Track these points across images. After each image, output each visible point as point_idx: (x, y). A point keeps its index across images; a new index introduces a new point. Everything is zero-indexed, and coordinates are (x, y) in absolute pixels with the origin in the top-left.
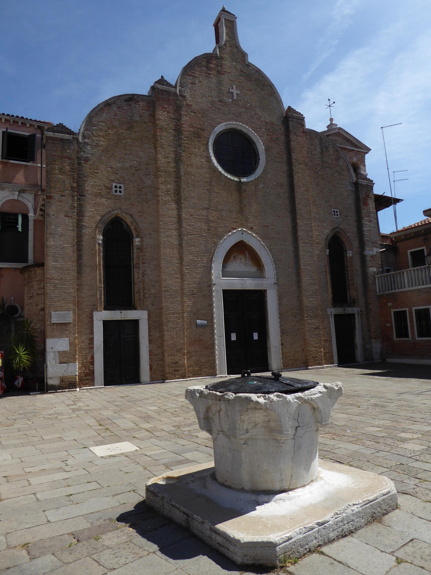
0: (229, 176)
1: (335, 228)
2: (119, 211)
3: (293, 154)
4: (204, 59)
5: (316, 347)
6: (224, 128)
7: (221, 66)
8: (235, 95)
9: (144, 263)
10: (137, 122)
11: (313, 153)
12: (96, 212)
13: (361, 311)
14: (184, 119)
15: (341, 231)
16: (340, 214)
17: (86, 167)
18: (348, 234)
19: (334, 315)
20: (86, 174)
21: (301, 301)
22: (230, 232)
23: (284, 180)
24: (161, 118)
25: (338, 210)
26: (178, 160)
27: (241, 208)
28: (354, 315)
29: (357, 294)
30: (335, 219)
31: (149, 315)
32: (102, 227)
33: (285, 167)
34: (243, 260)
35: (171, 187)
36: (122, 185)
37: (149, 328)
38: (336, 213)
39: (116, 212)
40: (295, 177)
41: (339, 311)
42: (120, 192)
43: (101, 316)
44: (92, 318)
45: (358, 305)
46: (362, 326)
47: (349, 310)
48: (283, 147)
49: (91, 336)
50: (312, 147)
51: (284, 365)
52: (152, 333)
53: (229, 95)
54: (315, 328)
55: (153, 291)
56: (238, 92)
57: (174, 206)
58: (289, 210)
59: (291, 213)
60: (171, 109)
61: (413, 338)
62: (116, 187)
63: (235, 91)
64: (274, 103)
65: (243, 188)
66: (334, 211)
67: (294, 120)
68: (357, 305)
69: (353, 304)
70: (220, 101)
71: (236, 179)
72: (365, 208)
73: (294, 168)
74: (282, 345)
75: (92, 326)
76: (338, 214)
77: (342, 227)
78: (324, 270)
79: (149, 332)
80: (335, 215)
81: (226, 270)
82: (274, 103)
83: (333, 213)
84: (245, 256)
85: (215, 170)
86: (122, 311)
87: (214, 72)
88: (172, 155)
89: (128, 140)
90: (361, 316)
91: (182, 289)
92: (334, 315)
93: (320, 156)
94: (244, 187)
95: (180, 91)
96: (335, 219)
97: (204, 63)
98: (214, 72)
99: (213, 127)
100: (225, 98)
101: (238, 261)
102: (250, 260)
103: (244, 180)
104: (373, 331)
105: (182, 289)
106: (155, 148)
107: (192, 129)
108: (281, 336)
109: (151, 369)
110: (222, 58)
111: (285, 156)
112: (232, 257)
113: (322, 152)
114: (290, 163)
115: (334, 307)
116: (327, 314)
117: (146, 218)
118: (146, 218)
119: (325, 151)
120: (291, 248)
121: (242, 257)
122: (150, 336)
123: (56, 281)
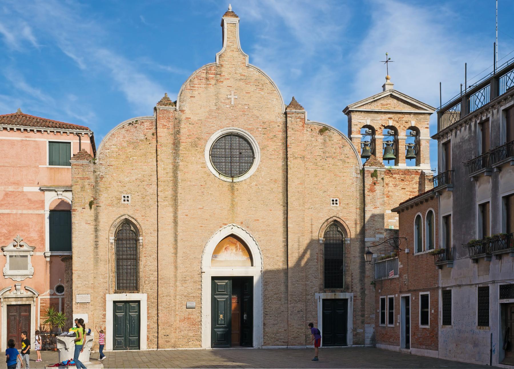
0: (222, 178)
1: (332, 217)
2: (127, 217)
3: (288, 149)
4: (204, 71)
5: (298, 328)
6: (221, 133)
7: (220, 74)
8: (233, 99)
9: (145, 257)
10: (142, 141)
11: (313, 145)
12: (110, 218)
13: (354, 297)
14: (182, 131)
15: (338, 220)
16: (340, 203)
17: (101, 185)
18: (347, 222)
19: (323, 300)
20: (101, 189)
21: (287, 287)
22: (220, 227)
23: (279, 175)
24: (162, 135)
25: (338, 199)
26: (176, 168)
27: (233, 205)
28: (346, 300)
29: (352, 280)
30: (334, 208)
31: (148, 297)
32: (113, 230)
33: (281, 163)
34: (234, 251)
35: (169, 193)
36: (129, 195)
37: (148, 308)
38: (335, 202)
39: (124, 217)
40: (289, 171)
41: (329, 295)
42: (128, 200)
43: (112, 297)
44: (105, 299)
45: (352, 291)
46: (354, 311)
47: (341, 296)
48: (280, 144)
49: (104, 313)
50: (313, 139)
51: (264, 343)
52: (150, 311)
53: (227, 101)
54: (298, 311)
55: (152, 278)
56: (236, 97)
57: (171, 209)
58: (281, 204)
59: (284, 206)
60: (170, 125)
61: (387, 324)
62: (124, 197)
63: (233, 97)
64: (273, 101)
65: (236, 187)
66: (333, 201)
67: (293, 115)
68: (350, 291)
69: (347, 289)
70: (218, 109)
71: (230, 180)
72: (371, 194)
73: (289, 163)
74: (264, 324)
75: (105, 305)
76: (338, 202)
77: (340, 215)
78: (316, 257)
79: (148, 310)
80: (333, 203)
81: (217, 259)
82: (273, 101)
83: (332, 202)
84: (236, 247)
85: (209, 174)
86: (128, 294)
87: (213, 82)
88: (171, 166)
89: (134, 158)
90: (354, 301)
91: (176, 276)
92: (323, 300)
93: (322, 147)
94: (236, 187)
95: (180, 107)
96: (334, 208)
97: (204, 75)
98: (213, 82)
99: (210, 134)
100: (222, 105)
101: (229, 252)
102: (240, 250)
103: (236, 180)
104: (366, 316)
105: (176, 276)
106: (157, 161)
107: (190, 140)
108: (265, 317)
109: (148, 339)
110: (222, 66)
111: (281, 152)
112: (224, 248)
113: (325, 142)
114: (286, 158)
115: (325, 292)
116: (314, 299)
117: (147, 220)
118: (147, 220)
119: (328, 140)
120: (281, 238)
121: (233, 247)
122: (148, 313)
123: (80, 272)
